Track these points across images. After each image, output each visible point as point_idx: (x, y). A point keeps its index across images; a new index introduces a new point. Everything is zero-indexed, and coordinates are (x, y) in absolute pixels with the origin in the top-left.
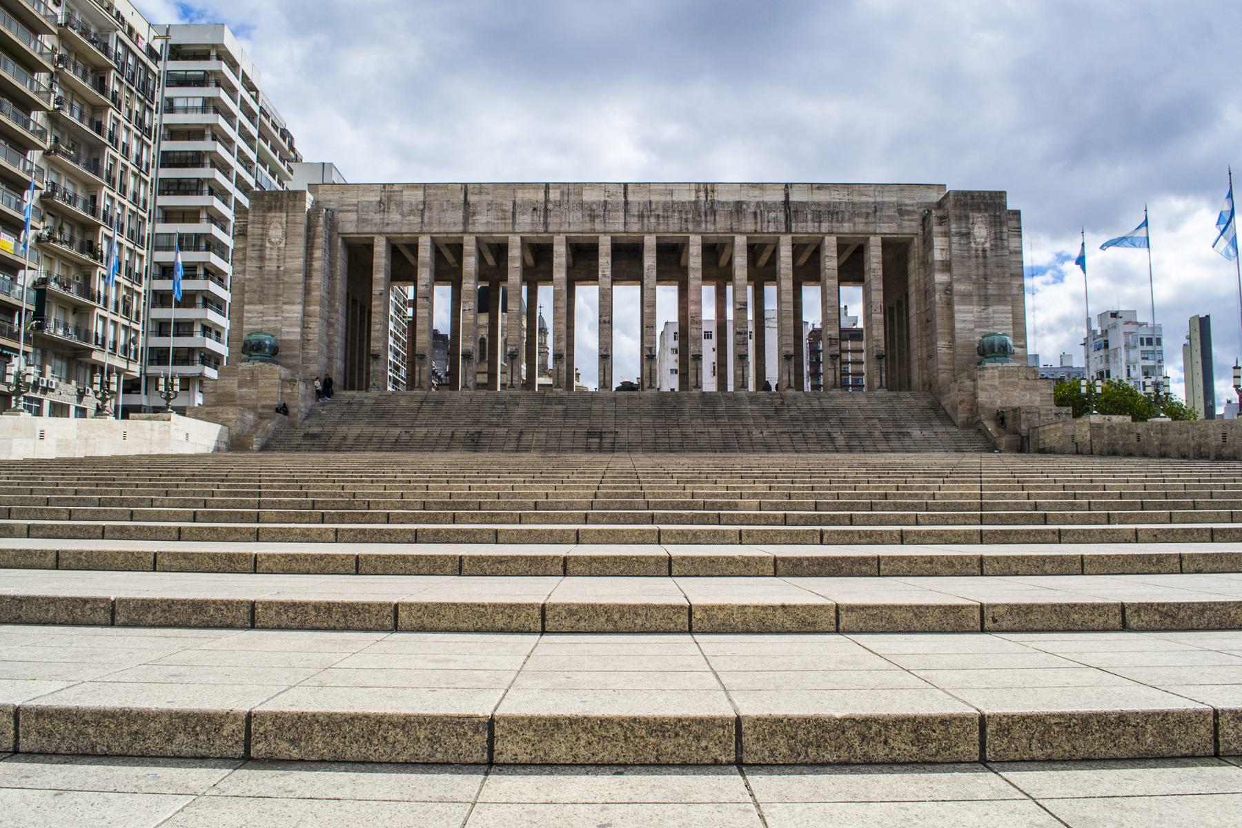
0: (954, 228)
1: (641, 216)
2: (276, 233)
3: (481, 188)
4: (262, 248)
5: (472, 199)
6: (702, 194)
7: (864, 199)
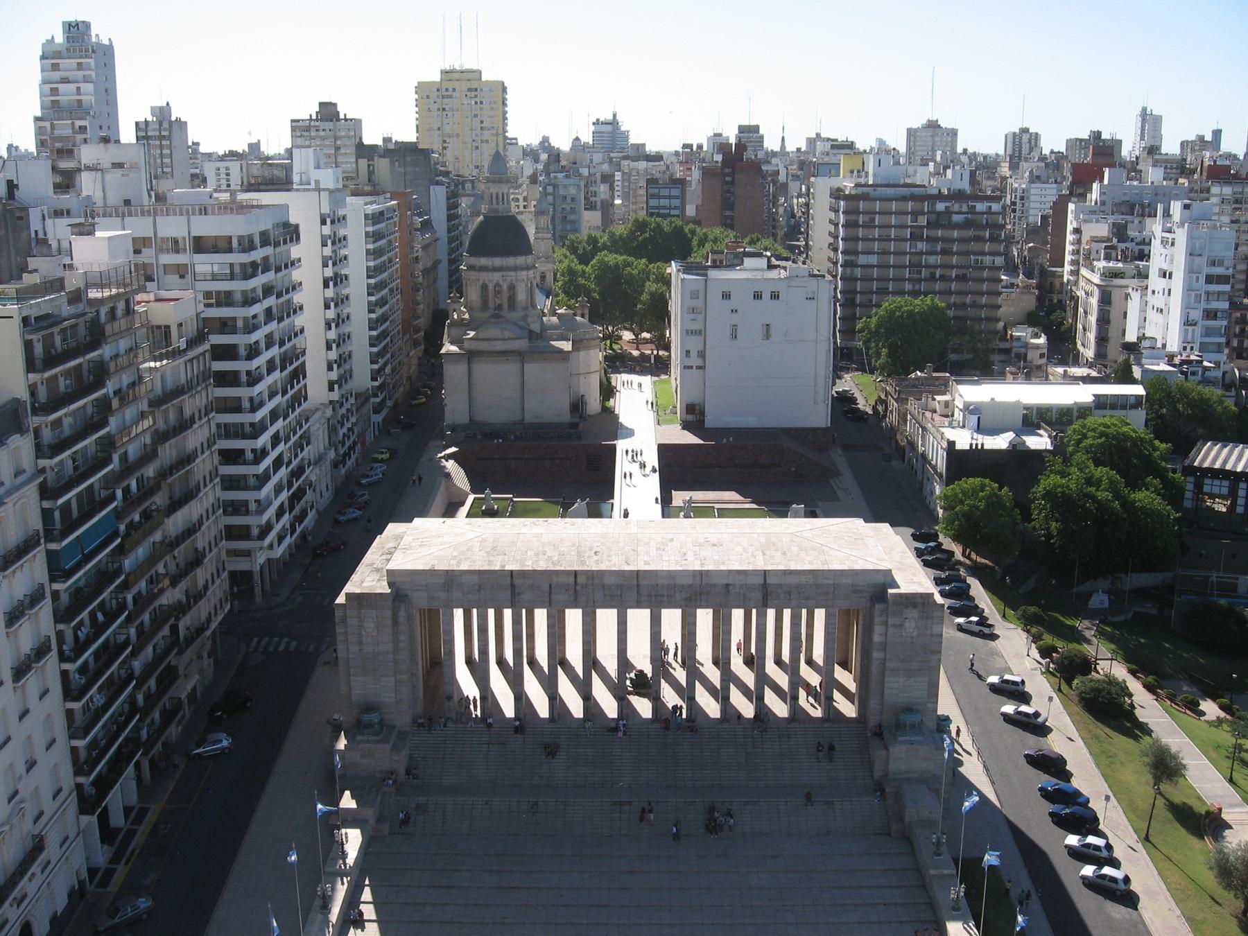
0: (891, 621)
1: (650, 596)
2: (369, 625)
3: (523, 574)
4: (360, 635)
5: (517, 582)
6: (698, 579)
7: (826, 581)
